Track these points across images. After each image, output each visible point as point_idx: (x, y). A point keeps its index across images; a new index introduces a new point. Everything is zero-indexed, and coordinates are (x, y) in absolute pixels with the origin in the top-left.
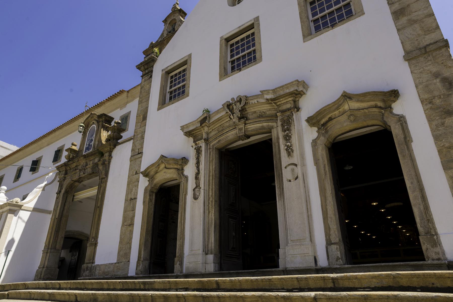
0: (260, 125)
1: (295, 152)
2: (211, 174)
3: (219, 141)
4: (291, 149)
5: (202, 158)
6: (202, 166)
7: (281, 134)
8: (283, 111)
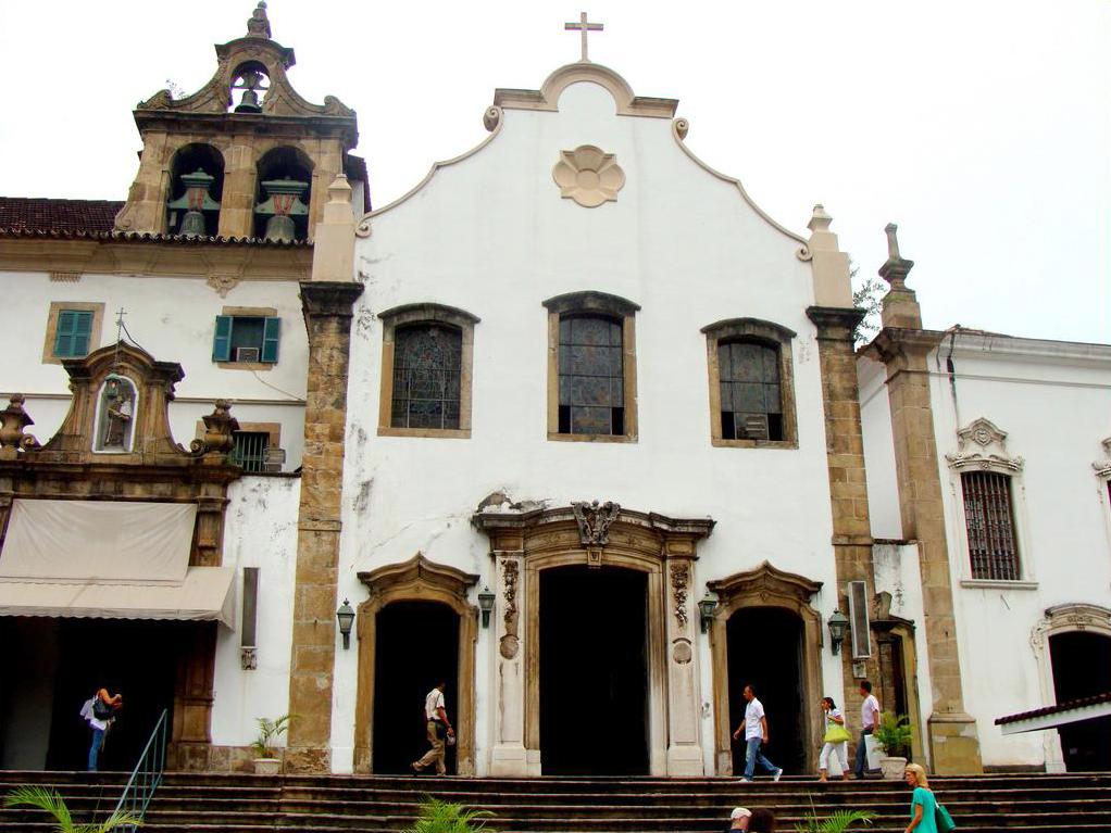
0: (631, 560)
1: (689, 622)
2: (532, 617)
3: (548, 563)
4: (685, 618)
5: (521, 585)
6: (520, 600)
7: (670, 590)
8: (677, 557)
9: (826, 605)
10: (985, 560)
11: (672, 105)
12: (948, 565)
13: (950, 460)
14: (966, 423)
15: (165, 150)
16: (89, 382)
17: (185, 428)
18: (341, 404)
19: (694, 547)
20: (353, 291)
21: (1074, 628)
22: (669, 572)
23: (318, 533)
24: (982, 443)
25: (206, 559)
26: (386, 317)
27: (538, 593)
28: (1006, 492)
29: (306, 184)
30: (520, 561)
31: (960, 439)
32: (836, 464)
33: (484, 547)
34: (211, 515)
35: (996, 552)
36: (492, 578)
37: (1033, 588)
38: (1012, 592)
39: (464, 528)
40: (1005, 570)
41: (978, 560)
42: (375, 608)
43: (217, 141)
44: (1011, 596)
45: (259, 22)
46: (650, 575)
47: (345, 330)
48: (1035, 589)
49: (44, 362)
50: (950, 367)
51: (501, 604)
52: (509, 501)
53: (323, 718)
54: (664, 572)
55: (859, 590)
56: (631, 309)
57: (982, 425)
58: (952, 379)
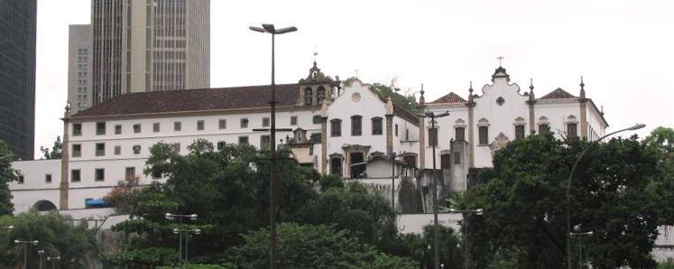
17: (308, 137)
34: (312, 149)
36: (344, 156)
45: (315, 64)
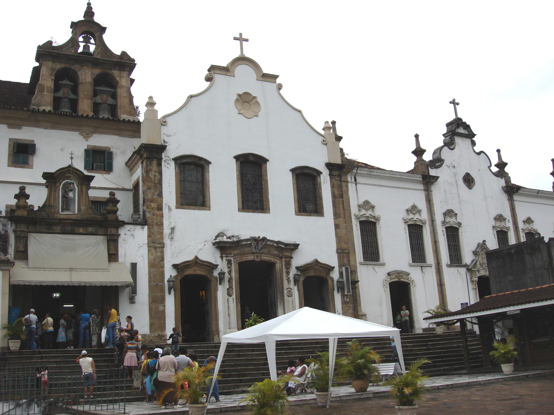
0: (269, 258)
1: (291, 282)
3: (241, 260)
4: (290, 280)
7: (284, 270)
8: (287, 257)
9: (335, 275)
10: (367, 254)
11: (276, 77)
12: (355, 256)
13: (356, 216)
14: (361, 201)
15: (52, 69)
16: (55, 183)
18: (160, 195)
19: (291, 254)
20: (162, 148)
21: (396, 280)
22: (284, 263)
23: (155, 248)
24: (366, 210)
25: (112, 259)
26: (176, 160)
27: (238, 271)
28: (374, 228)
29: (113, 90)
30: (232, 259)
31: (359, 208)
32: (337, 223)
33: (218, 254)
35: (371, 251)
36: (222, 265)
37: (383, 265)
38: (377, 266)
39: (210, 246)
40: (374, 258)
41: (365, 254)
42: (180, 278)
43: (76, 67)
44: (377, 268)
45: (89, 13)
46: (276, 264)
47: (160, 165)
48: (384, 265)
49: (8, 166)
50: (355, 180)
51: (227, 275)
52: (226, 235)
53: (162, 322)
54: (282, 263)
55: (347, 270)
56: (265, 161)
57: (367, 203)
58: (356, 184)
